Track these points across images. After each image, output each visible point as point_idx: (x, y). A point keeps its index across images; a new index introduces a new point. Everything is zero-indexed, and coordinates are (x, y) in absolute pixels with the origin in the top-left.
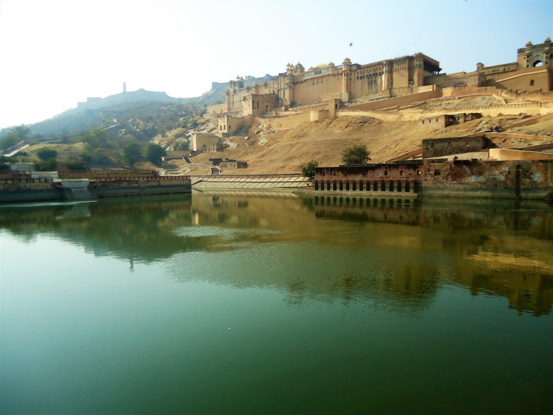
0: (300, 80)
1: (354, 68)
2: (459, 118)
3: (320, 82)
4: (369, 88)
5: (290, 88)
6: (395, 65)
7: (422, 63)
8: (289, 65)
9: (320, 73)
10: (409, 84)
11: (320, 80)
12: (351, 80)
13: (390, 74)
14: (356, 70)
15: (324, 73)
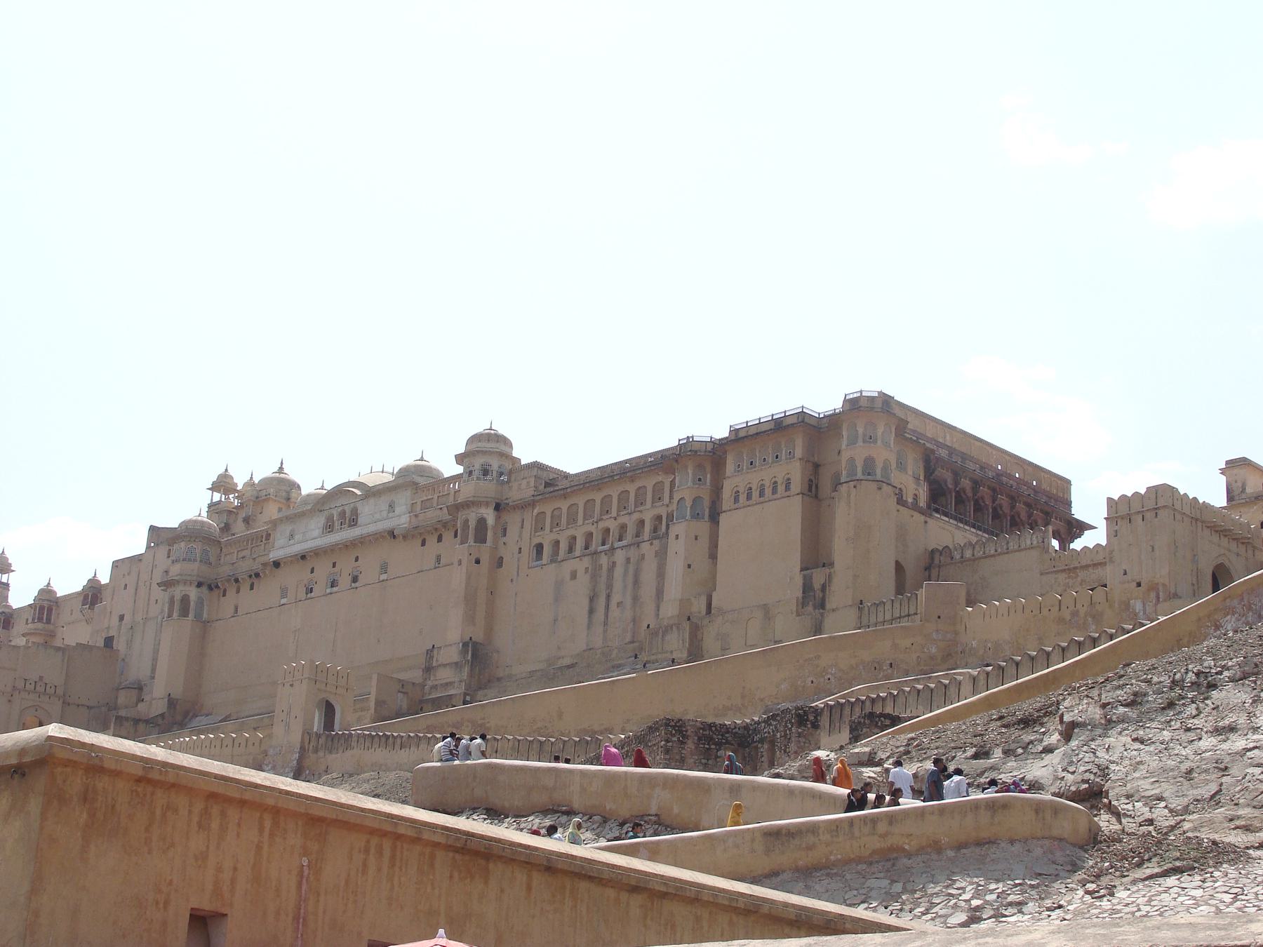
0: (245, 567)
1: (521, 491)
2: (772, 743)
3: (345, 581)
4: (591, 611)
5: (184, 612)
6: (730, 467)
7: (884, 454)
8: (223, 484)
9: (354, 522)
10: (807, 587)
11: (346, 566)
12: (500, 562)
13: (703, 527)
14: (531, 504)
15: (372, 519)
